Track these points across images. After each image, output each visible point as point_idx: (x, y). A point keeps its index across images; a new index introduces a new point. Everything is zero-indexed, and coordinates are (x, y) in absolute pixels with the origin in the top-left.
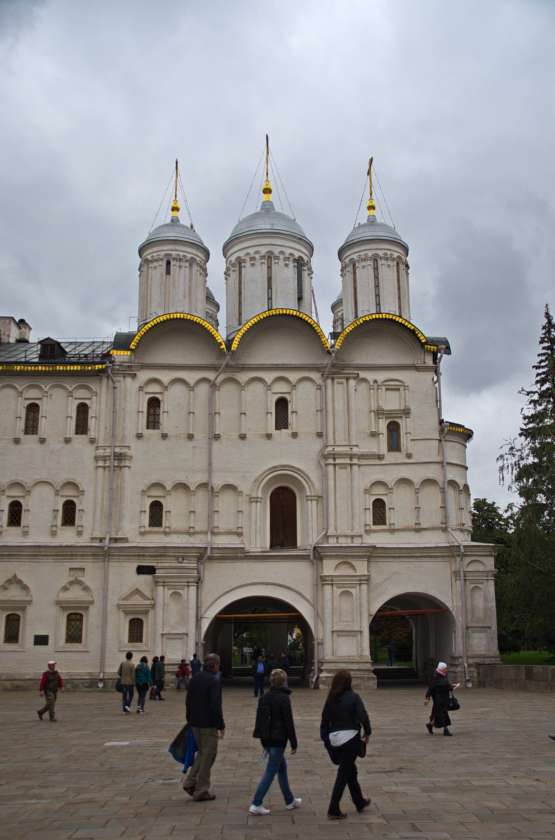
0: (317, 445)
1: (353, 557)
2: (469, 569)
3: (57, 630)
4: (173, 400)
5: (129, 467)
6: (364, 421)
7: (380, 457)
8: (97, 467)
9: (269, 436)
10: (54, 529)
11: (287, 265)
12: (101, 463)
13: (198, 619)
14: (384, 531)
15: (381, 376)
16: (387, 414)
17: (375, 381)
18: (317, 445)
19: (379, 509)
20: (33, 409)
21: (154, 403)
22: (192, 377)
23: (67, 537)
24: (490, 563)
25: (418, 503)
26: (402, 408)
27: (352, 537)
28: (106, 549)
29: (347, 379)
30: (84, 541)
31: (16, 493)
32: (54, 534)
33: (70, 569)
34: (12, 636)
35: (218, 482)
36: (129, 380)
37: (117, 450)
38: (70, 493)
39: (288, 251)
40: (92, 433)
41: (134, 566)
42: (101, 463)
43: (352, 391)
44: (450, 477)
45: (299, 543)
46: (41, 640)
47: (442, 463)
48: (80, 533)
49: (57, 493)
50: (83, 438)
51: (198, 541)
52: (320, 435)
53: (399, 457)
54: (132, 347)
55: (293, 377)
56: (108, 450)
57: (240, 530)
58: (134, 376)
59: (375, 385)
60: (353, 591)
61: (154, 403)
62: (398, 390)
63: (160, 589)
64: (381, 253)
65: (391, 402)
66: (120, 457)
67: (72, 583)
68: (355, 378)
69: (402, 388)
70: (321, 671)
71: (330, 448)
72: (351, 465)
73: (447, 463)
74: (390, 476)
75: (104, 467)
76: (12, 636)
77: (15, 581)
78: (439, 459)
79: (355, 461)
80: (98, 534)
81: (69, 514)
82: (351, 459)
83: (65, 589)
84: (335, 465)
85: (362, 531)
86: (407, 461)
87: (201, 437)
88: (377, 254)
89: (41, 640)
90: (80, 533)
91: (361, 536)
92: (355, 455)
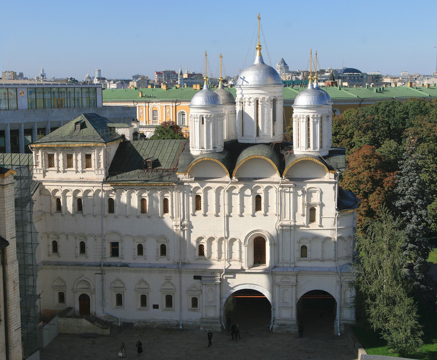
1: (289, 275)
3: (162, 303)
10: (157, 258)
13: (221, 299)
30: (171, 262)
31: (140, 241)
38: (163, 242)
41: (193, 275)
46: (156, 307)
49: (157, 241)
60: (289, 289)
63: (204, 287)
70: (273, 324)
77: (143, 281)
80: (176, 260)
81: (163, 250)
89: (156, 307)
90: (169, 260)
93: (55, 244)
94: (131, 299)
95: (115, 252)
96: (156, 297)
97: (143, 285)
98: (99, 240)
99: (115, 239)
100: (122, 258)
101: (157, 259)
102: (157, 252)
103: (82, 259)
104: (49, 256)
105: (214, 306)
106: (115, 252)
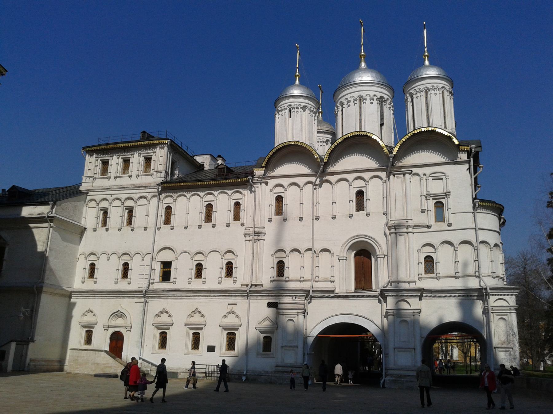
0: (384, 219)
2: (496, 304)
3: (221, 342)
4: (291, 197)
5: (264, 240)
6: (416, 202)
7: (429, 227)
8: (245, 241)
9: (351, 216)
11: (372, 103)
12: (248, 238)
14: (432, 278)
15: (428, 170)
16: (435, 197)
17: (425, 175)
18: (384, 219)
19: (429, 262)
20: (209, 207)
21: (279, 199)
22: (301, 181)
23: (228, 284)
24: (512, 300)
25: (456, 257)
26: (445, 192)
27: (409, 282)
28: (248, 291)
29: (404, 175)
30: (237, 286)
31: (199, 257)
32: (220, 282)
33: (229, 304)
34: (196, 344)
35: (318, 248)
36: (264, 185)
37: (256, 229)
39: (372, 94)
40: (242, 220)
42: (248, 238)
43: (408, 182)
44: (481, 239)
45: (374, 288)
46: (211, 349)
47: (475, 229)
48: (235, 282)
50: (238, 223)
51: (306, 286)
52: (385, 214)
53: (444, 226)
54: (263, 165)
55: (366, 176)
56: (252, 230)
57: (332, 278)
58: (267, 183)
59: (425, 177)
61: (279, 199)
62: (442, 179)
64: (429, 86)
65: (436, 188)
66: (258, 234)
67: (229, 313)
68: (410, 174)
69: (444, 178)
71: (393, 222)
72: (407, 233)
73: (479, 229)
74: (436, 239)
75: (249, 240)
76: (196, 344)
78: (473, 226)
79: (410, 230)
81: (229, 269)
82: (407, 228)
83: (225, 316)
84: (396, 233)
85: (416, 279)
86: (449, 228)
87: (308, 219)
88: (427, 87)
89: (211, 349)
90: (235, 282)
91: (415, 282)
92: (409, 226)
93: (93, 267)
94: (179, 338)
95: (166, 276)
96: (213, 335)
97: (197, 319)
98: (148, 258)
99: (166, 256)
100: (175, 283)
101: (220, 282)
102: (221, 272)
103: (123, 285)
104: (83, 282)
105: (295, 347)
106: (166, 276)
